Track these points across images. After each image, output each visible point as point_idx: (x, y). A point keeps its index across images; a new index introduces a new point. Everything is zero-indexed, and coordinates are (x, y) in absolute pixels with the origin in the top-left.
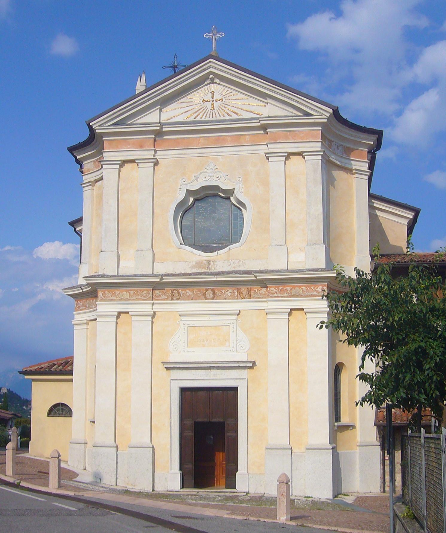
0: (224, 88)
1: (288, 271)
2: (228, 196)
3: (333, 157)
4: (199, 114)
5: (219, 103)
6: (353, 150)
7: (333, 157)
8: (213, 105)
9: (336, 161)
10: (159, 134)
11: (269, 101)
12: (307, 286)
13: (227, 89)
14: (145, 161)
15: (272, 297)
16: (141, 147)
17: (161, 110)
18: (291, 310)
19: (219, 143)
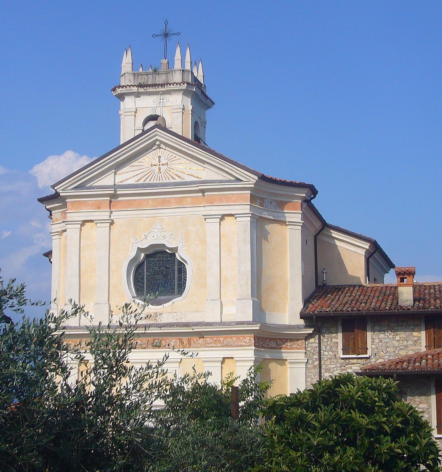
0: (169, 153)
1: (222, 323)
2: (173, 252)
3: (266, 213)
4: (148, 177)
5: (165, 167)
6: (286, 203)
7: (266, 213)
8: (160, 169)
9: (268, 217)
10: (114, 197)
11: (206, 166)
12: (237, 337)
13: (171, 154)
14: (102, 221)
15: (208, 347)
16: (99, 208)
17: (115, 173)
18: (224, 358)
19: (164, 205)
